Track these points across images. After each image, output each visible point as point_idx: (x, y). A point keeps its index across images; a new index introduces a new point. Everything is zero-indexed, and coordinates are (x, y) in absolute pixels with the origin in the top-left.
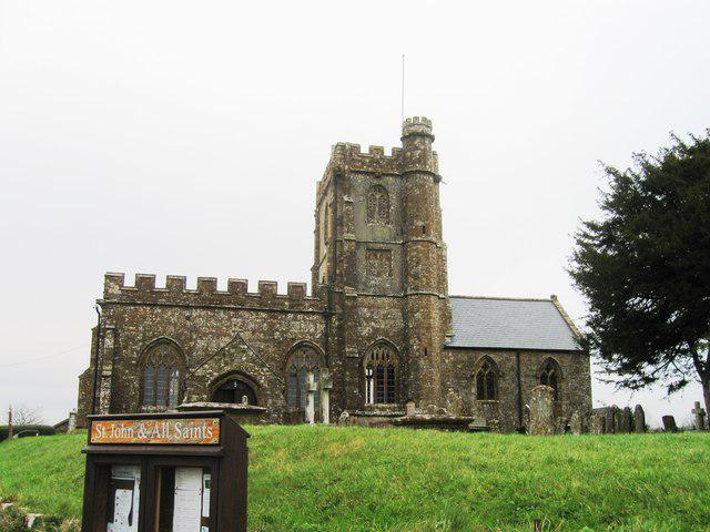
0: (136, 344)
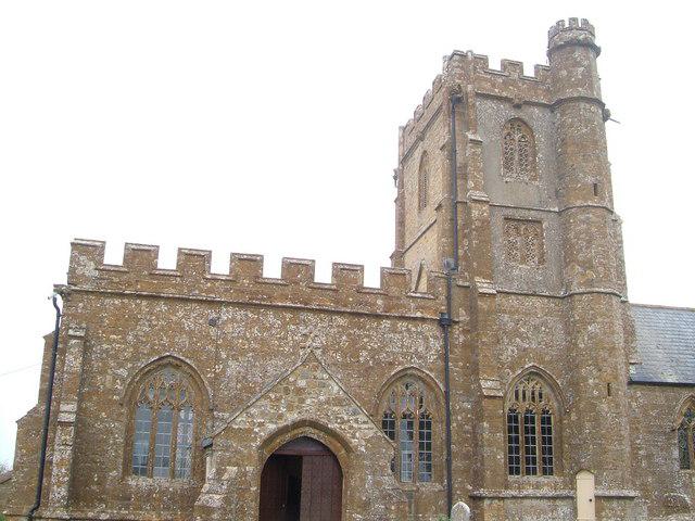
0: (121, 365)
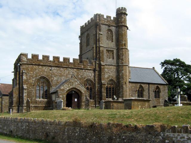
0: (33, 78)
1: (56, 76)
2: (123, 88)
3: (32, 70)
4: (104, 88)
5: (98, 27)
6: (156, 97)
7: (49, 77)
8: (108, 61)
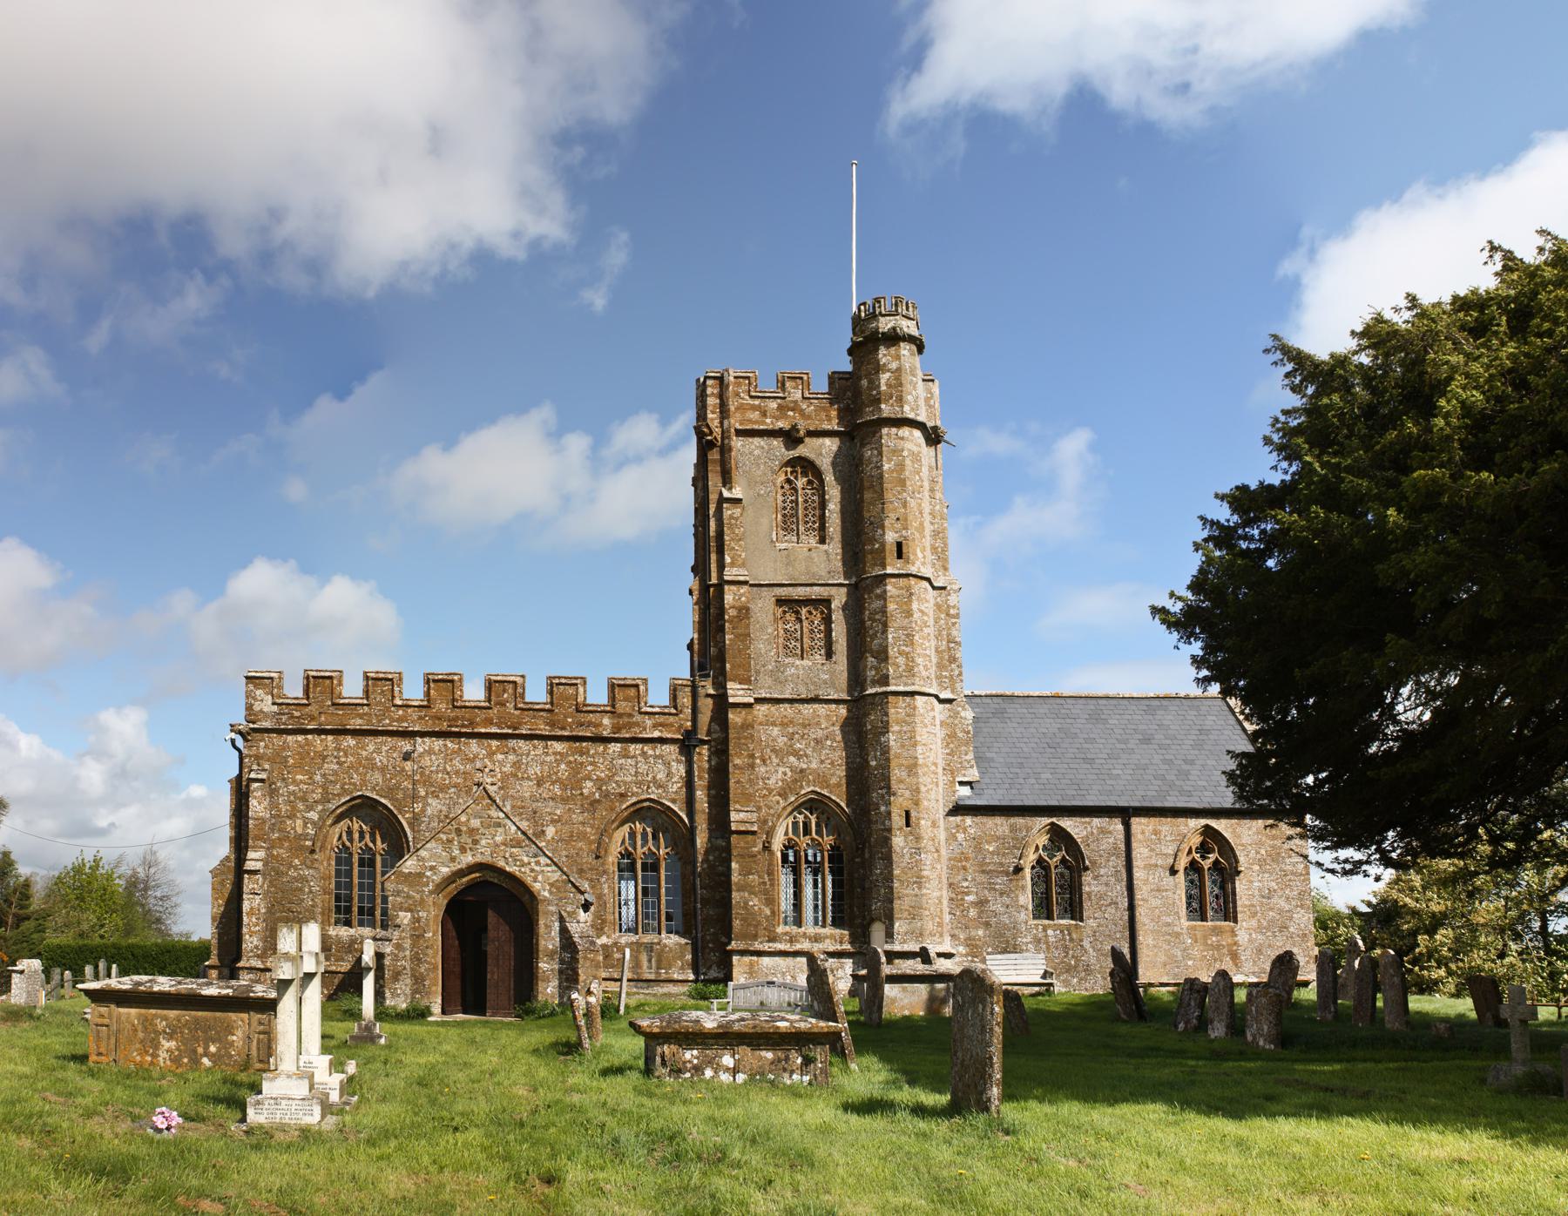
0: (310, 808)
1: (439, 790)
2: (888, 858)
3: (309, 761)
4: (742, 856)
5: (714, 455)
6: (1197, 909)
7: (400, 796)
8: (685, 682)
